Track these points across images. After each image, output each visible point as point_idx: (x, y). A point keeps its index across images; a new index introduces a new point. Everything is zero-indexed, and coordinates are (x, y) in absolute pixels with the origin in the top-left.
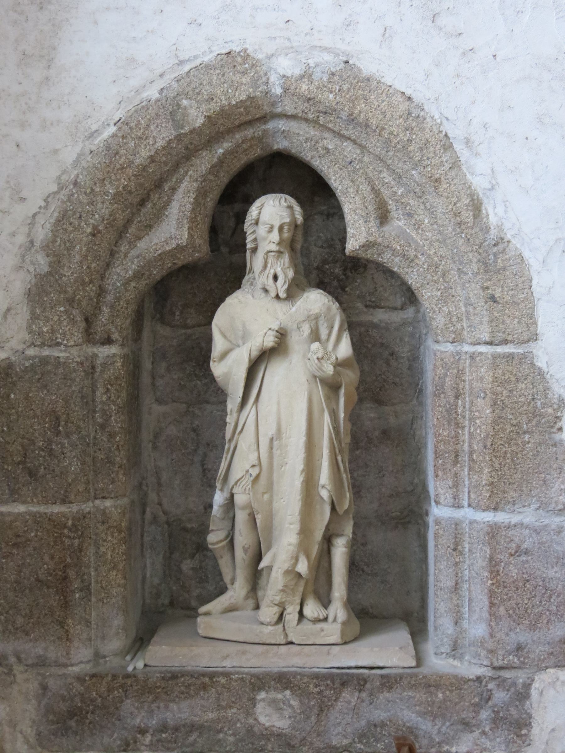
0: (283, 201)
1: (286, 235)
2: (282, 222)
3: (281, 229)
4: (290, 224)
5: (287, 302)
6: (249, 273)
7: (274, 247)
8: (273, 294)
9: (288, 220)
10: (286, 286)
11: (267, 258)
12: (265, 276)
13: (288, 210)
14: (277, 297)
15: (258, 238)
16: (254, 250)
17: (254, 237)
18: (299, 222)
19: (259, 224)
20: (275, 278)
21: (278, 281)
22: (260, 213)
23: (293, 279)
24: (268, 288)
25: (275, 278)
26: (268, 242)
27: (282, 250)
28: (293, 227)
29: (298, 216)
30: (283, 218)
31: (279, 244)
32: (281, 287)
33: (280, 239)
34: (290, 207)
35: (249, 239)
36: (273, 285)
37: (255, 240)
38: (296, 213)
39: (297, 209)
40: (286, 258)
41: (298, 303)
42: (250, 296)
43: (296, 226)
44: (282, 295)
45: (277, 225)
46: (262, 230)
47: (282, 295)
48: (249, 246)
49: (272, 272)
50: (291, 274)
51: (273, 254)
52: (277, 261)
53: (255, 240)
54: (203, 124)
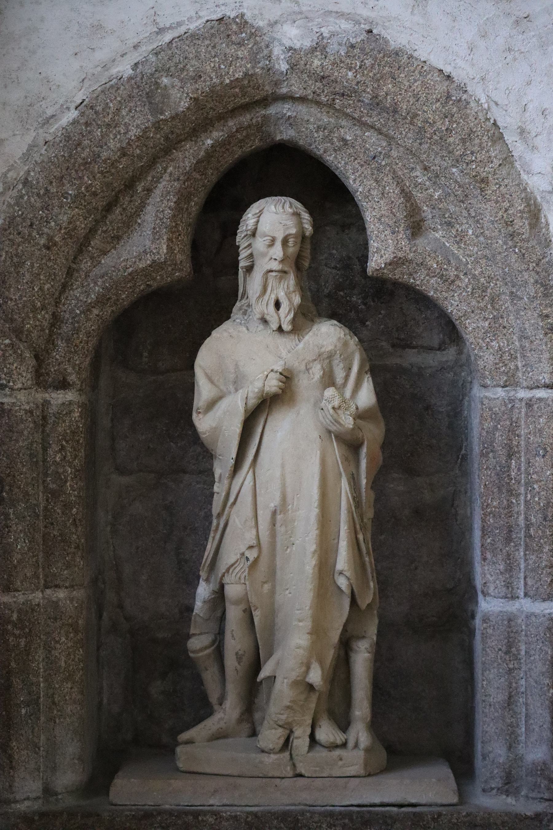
0: (287, 206)
1: (292, 249)
2: (287, 233)
3: (285, 242)
4: (295, 236)
5: (292, 337)
6: (242, 297)
7: (275, 266)
8: (275, 326)
9: (293, 231)
10: (292, 315)
11: (267, 279)
12: (265, 302)
13: (294, 218)
14: (280, 329)
15: (254, 254)
16: (250, 269)
17: (249, 252)
18: (307, 234)
19: (256, 235)
20: (278, 305)
21: (281, 309)
22: (258, 222)
23: (300, 306)
24: (268, 318)
25: (278, 305)
26: (267, 258)
27: (286, 269)
29: (306, 226)
30: (288, 228)
31: (282, 261)
32: (286, 316)
33: (284, 255)
34: (297, 214)
35: (243, 254)
36: (275, 315)
37: (251, 255)
38: (305, 221)
39: (306, 216)
40: (291, 280)
41: (307, 337)
42: (244, 329)
43: (304, 237)
44: (287, 327)
45: (280, 237)
46: (260, 244)
47: (287, 327)
48: (242, 264)
49: (273, 297)
50: (297, 300)
51: (274, 274)
52: (280, 282)
53: (251, 255)
54: (188, 109)
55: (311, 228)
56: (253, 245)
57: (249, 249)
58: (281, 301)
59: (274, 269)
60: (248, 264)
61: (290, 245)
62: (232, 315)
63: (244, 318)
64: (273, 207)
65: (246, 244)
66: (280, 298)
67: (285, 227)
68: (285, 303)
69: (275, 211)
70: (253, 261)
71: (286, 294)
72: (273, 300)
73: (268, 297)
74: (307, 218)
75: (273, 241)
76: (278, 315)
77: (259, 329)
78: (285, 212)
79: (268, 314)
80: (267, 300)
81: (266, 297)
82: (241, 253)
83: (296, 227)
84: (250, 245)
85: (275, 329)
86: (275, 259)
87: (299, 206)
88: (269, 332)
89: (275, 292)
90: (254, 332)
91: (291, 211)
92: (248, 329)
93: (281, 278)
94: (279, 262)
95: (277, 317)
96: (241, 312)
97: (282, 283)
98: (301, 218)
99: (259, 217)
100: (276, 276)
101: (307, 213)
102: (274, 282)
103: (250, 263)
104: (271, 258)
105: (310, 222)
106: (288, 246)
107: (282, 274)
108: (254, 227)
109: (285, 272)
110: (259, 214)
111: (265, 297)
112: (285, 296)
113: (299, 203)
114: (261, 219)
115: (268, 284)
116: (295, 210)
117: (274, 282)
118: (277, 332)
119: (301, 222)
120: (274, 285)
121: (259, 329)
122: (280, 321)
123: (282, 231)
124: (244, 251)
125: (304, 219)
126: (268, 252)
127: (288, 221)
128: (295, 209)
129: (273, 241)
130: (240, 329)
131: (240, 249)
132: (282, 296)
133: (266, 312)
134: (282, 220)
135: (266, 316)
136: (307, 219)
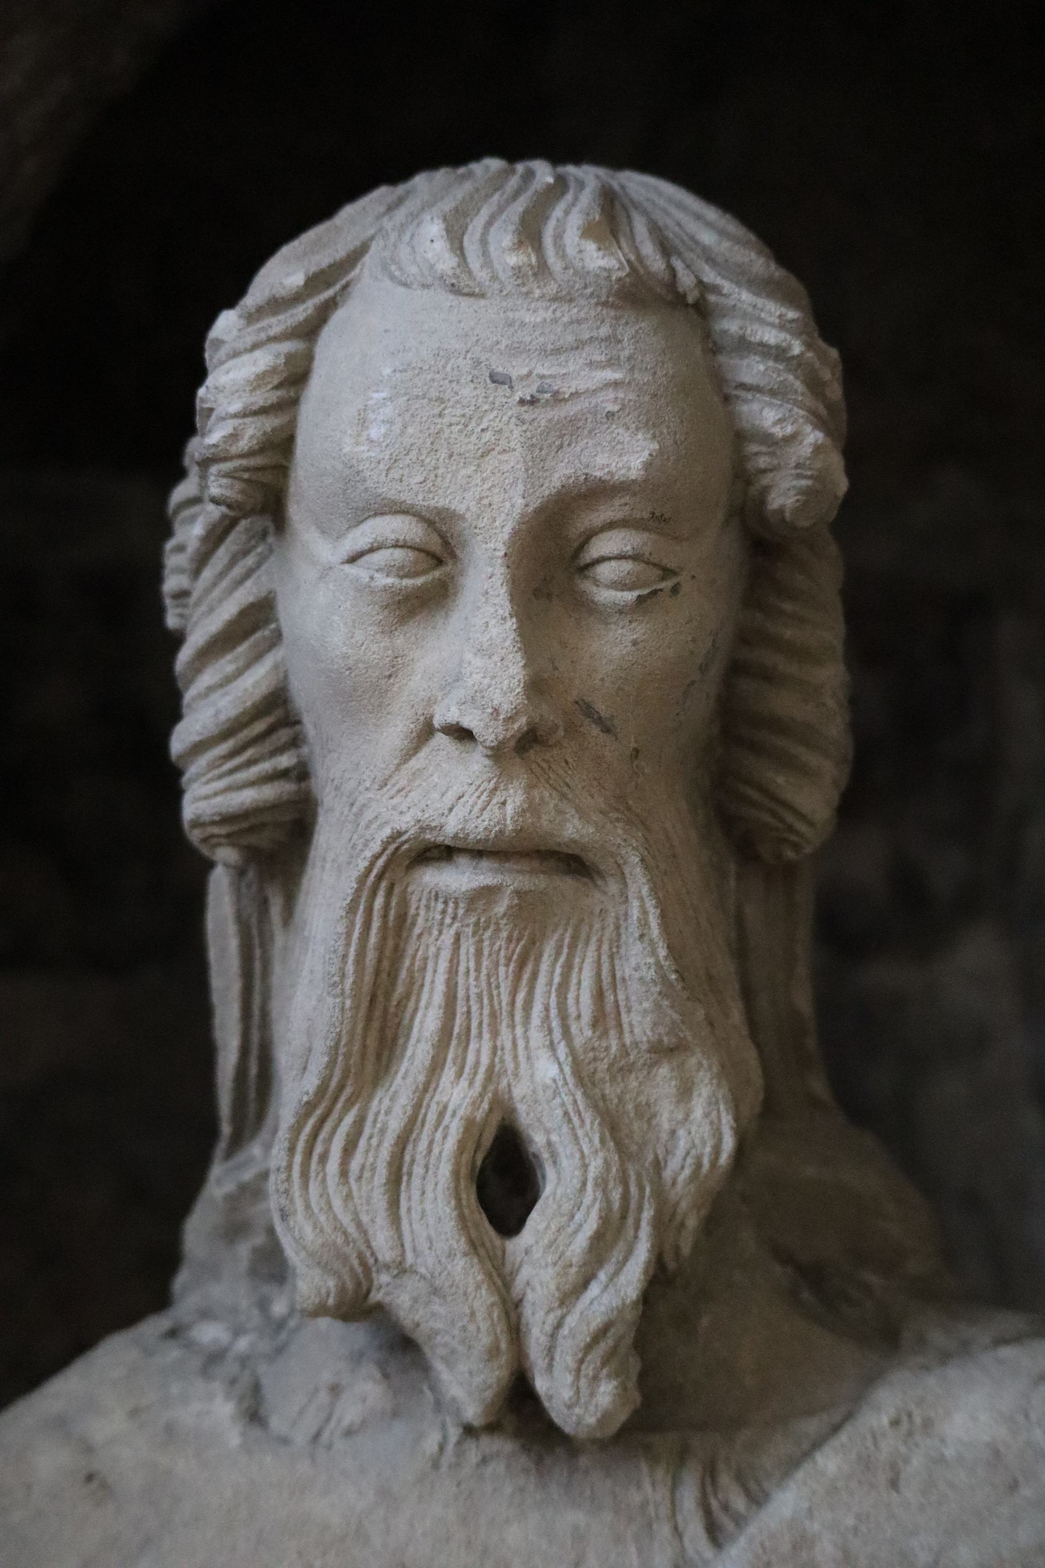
0: (569, 223)
1: (616, 646)
2: (562, 472)
3: (550, 563)
4: (656, 503)
5: (647, 1488)
7: (458, 793)
8: (467, 1383)
9: (626, 454)
10: (627, 1280)
11: (398, 928)
12: (375, 1155)
13: (638, 333)
14: (519, 1410)
15: (304, 694)
17: (255, 682)
18: (784, 495)
19: (295, 511)
20: (503, 1179)
21: (538, 1222)
22: (296, 377)
23: (741, 1192)
24: (403, 1300)
25: (503, 1179)
26: (395, 732)
27: (573, 830)
28: (708, 554)
29: (767, 416)
30: (569, 431)
31: (525, 747)
32: (573, 1284)
33: (536, 686)
34: (667, 302)
35: (211, 701)
36: (464, 1272)
37: (276, 716)
38: (753, 370)
39: (765, 322)
40: (632, 942)
42: (223, 1410)
43: (762, 546)
44: (579, 1394)
45: (494, 513)
46: (327, 588)
47: (579, 1394)
48: (207, 796)
49: (458, 1097)
50: (697, 1126)
51: (458, 879)
52: (525, 960)
53: (276, 716)
55: (813, 436)
56: (287, 613)
57: (257, 657)
58: (538, 1141)
59: (452, 826)
60: (248, 797)
61: (605, 596)
62: (181, 1279)
63: (263, 1305)
64: (433, 228)
65: (229, 610)
66: (525, 1118)
67: (544, 416)
68: (569, 1164)
69: (447, 263)
70: (302, 773)
71: (583, 1075)
72: (455, 1128)
73: (405, 1100)
74: (771, 336)
75: (434, 566)
76: (501, 1279)
77: (350, 1412)
78: (542, 269)
79: (401, 1269)
80: (395, 1125)
81: (391, 1105)
82: (188, 696)
83: (651, 424)
84: (257, 622)
85: (473, 1412)
86: (462, 734)
87: (707, 238)
88: (431, 1443)
89: (480, 1050)
90: (301, 1438)
91: (597, 260)
92: (254, 1415)
93: (531, 922)
94: (497, 754)
95: (484, 1299)
96: (244, 1250)
97: (548, 967)
98: (713, 345)
99: (310, 331)
100: (486, 894)
101: (788, 299)
102: (468, 946)
103: (268, 793)
104: (426, 731)
105: (815, 385)
106: (584, 607)
107: (540, 882)
108: (252, 432)
109: (575, 864)
110: (302, 312)
111: (380, 1102)
112: (572, 1096)
113: (712, 213)
114: (332, 350)
115: (414, 987)
116: (657, 264)
117: (468, 946)
118: (502, 1445)
119: (718, 379)
120: (469, 985)
121: (350, 1412)
122: (516, 1331)
123: (514, 460)
124: (207, 678)
125: (744, 346)
126: (394, 669)
127: (574, 363)
128: (648, 249)
129: (434, 566)
130: (187, 1415)
131: (185, 655)
132: (542, 1086)
133: (382, 1240)
134: (516, 350)
135: (386, 1290)
136: (779, 354)
